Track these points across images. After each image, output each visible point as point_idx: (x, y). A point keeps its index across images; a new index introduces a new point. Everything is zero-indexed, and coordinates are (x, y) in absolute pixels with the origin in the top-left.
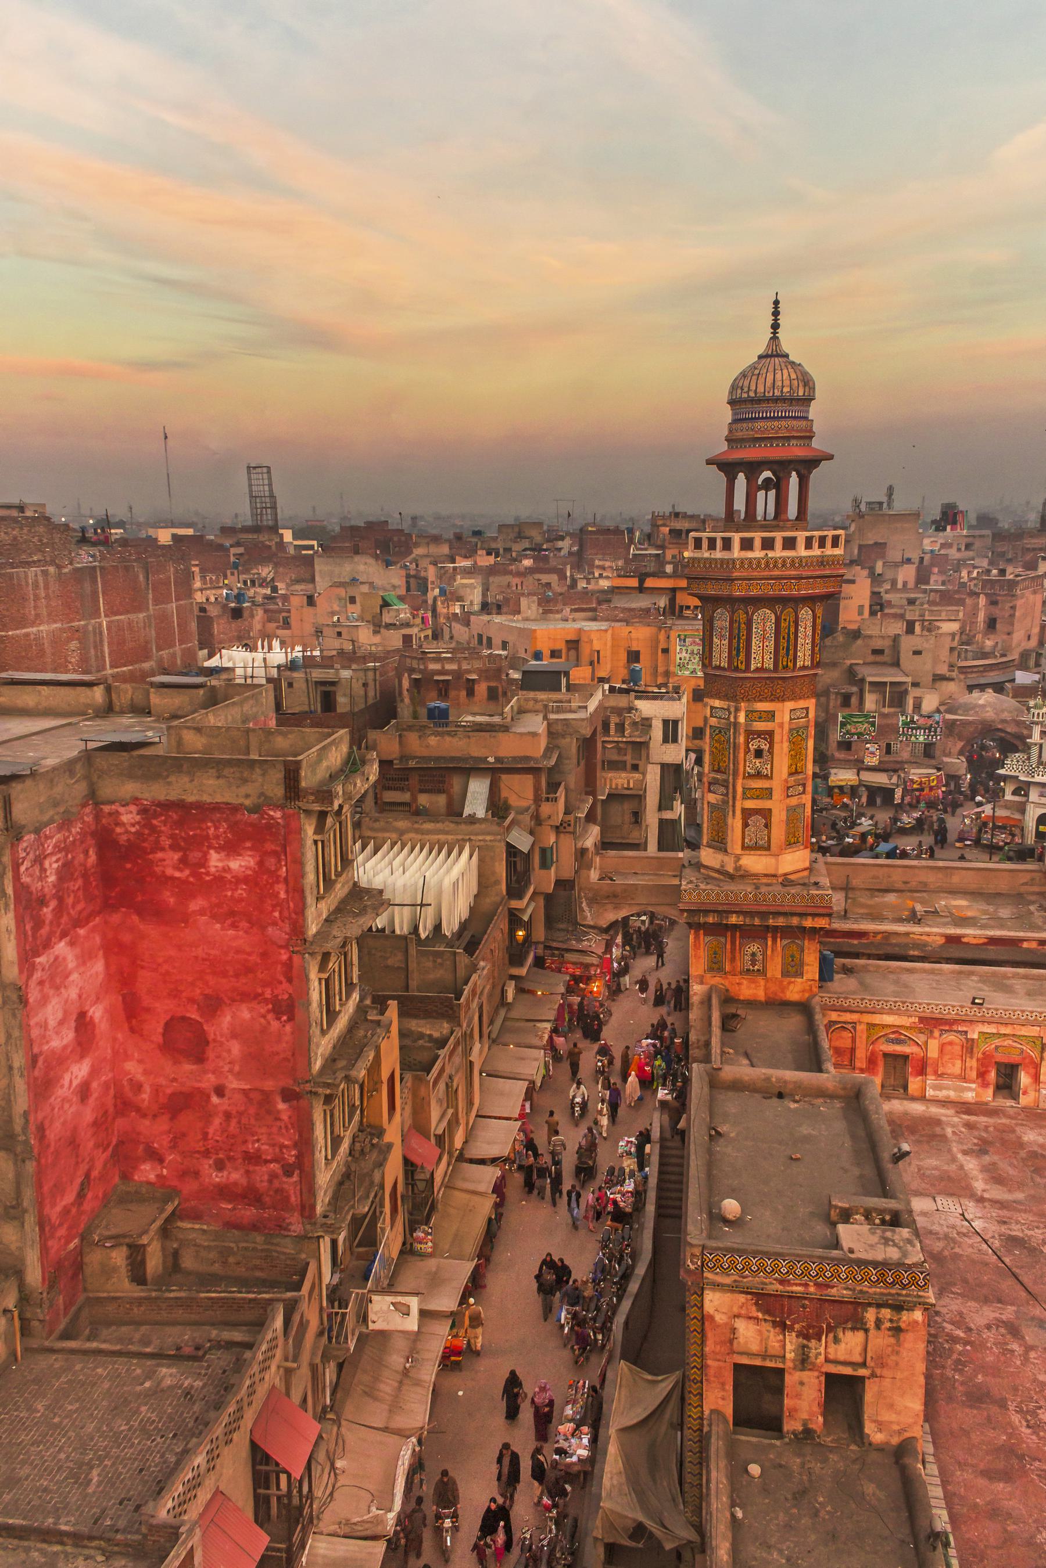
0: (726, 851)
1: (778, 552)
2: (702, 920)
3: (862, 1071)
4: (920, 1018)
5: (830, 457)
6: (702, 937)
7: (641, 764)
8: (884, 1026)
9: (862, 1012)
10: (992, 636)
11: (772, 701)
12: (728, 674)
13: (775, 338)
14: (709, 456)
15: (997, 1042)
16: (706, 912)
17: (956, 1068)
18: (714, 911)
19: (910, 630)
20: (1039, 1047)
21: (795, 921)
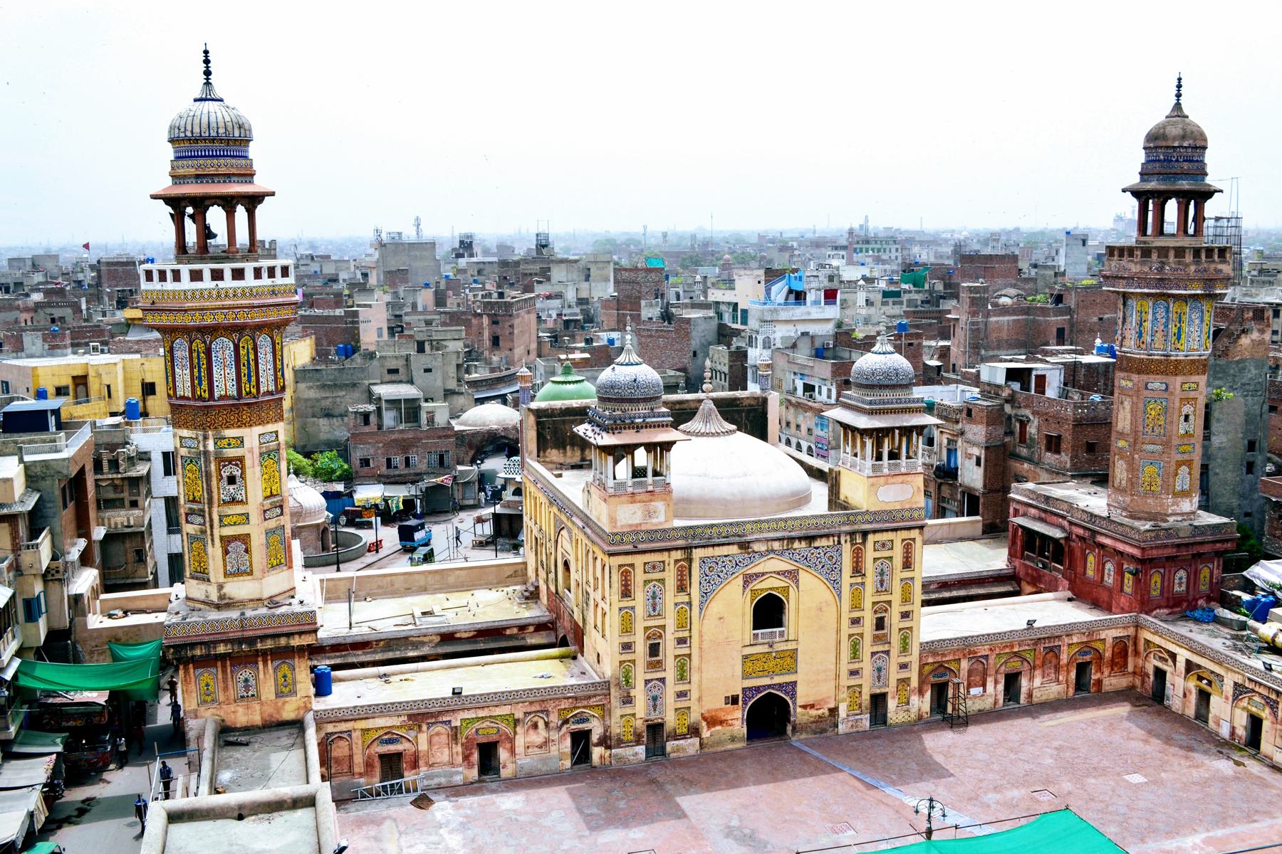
0: (209, 580)
1: (228, 283)
2: (189, 654)
3: (361, 775)
4: (410, 717)
5: (273, 194)
6: (192, 670)
7: (140, 500)
8: (377, 729)
9: (355, 720)
10: (497, 353)
11: (239, 427)
12: (192, 403)
13: (208, 83)
14: (155, 191)
15: (477, 725)
16: (193, 645)
17: (444, 756)
18: (201, 643)
19: (421, 349)
20: (512, 724)
21: (283, 641)
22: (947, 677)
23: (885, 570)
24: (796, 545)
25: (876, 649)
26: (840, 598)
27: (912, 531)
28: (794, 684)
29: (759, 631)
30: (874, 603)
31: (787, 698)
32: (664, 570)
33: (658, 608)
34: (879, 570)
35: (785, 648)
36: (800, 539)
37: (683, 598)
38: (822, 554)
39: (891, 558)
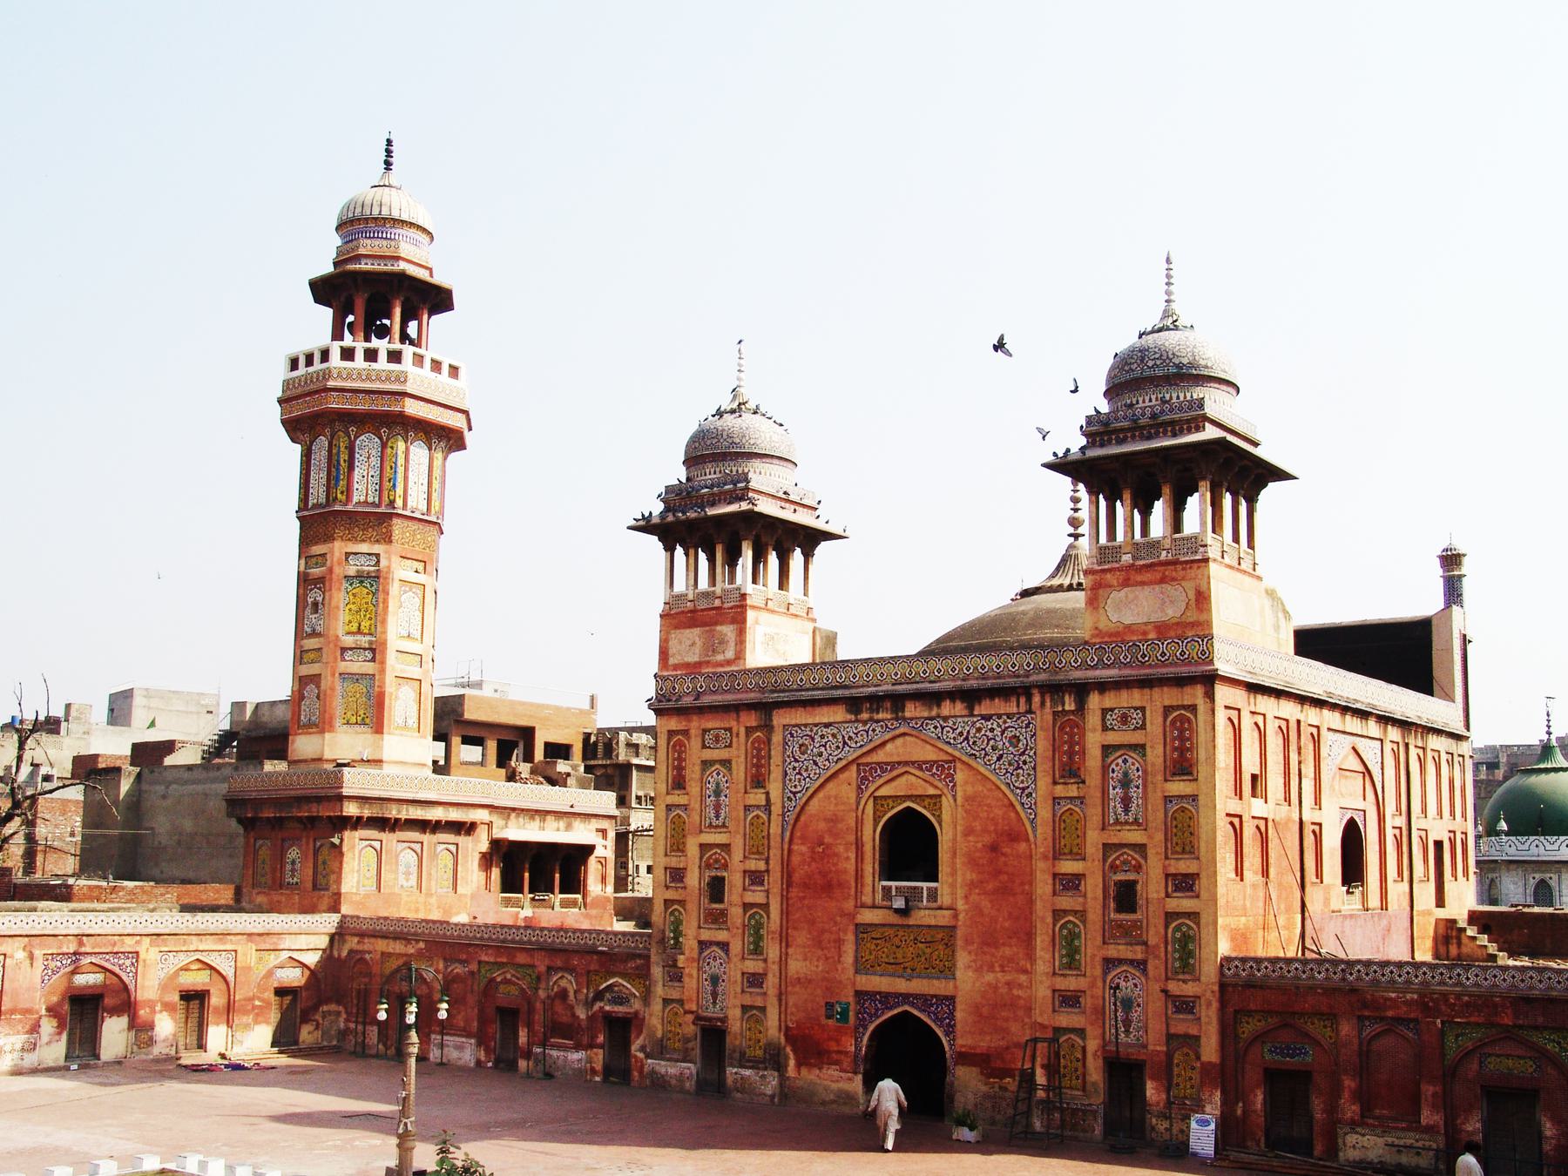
22: (1309, 1059)
23: (1133, 774)
24: (947, 708)
25: (1113, 951)
26: (1034, 829)
27: (1188, 690)
28: (951, 999)
29: (893, 884)
30: (1108, 848)
31: (939, 1032)
32: (730, 746)
33: (723, 815)
34: (1118, 775)
35: (933, 922)
36: (952, 695)
37: (757, 797)
38: (998, 731)
39: (1143, 747)
